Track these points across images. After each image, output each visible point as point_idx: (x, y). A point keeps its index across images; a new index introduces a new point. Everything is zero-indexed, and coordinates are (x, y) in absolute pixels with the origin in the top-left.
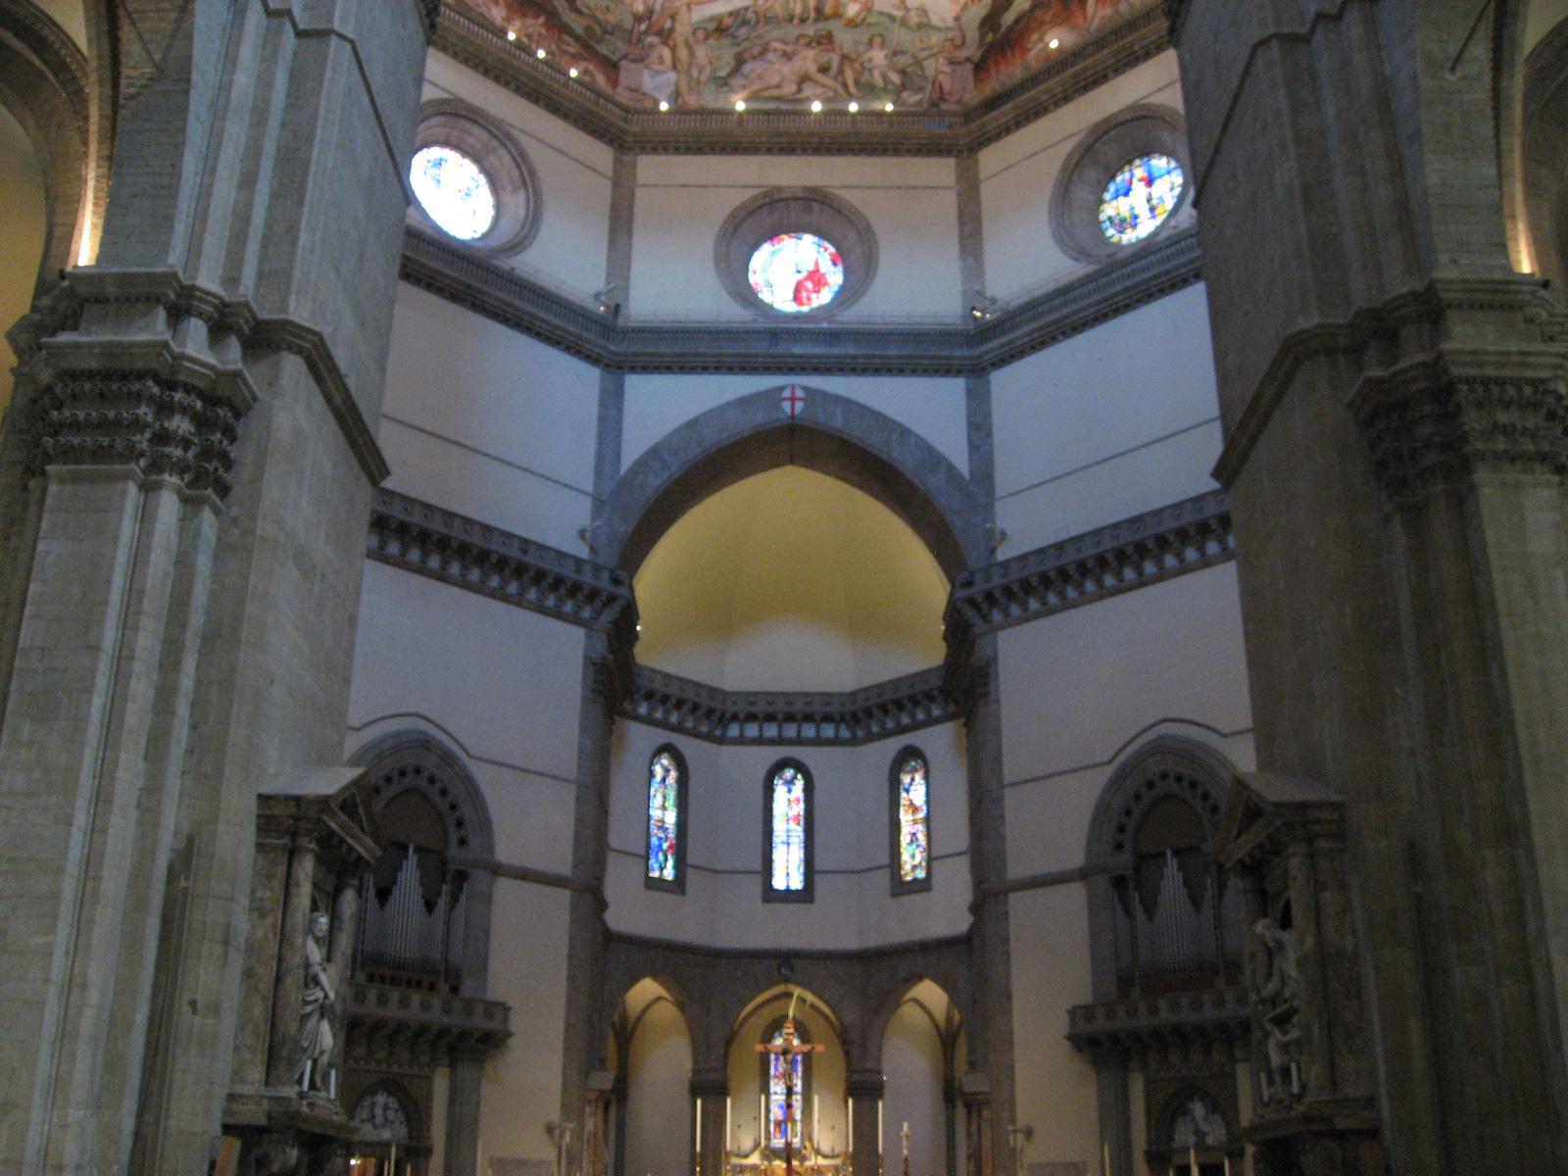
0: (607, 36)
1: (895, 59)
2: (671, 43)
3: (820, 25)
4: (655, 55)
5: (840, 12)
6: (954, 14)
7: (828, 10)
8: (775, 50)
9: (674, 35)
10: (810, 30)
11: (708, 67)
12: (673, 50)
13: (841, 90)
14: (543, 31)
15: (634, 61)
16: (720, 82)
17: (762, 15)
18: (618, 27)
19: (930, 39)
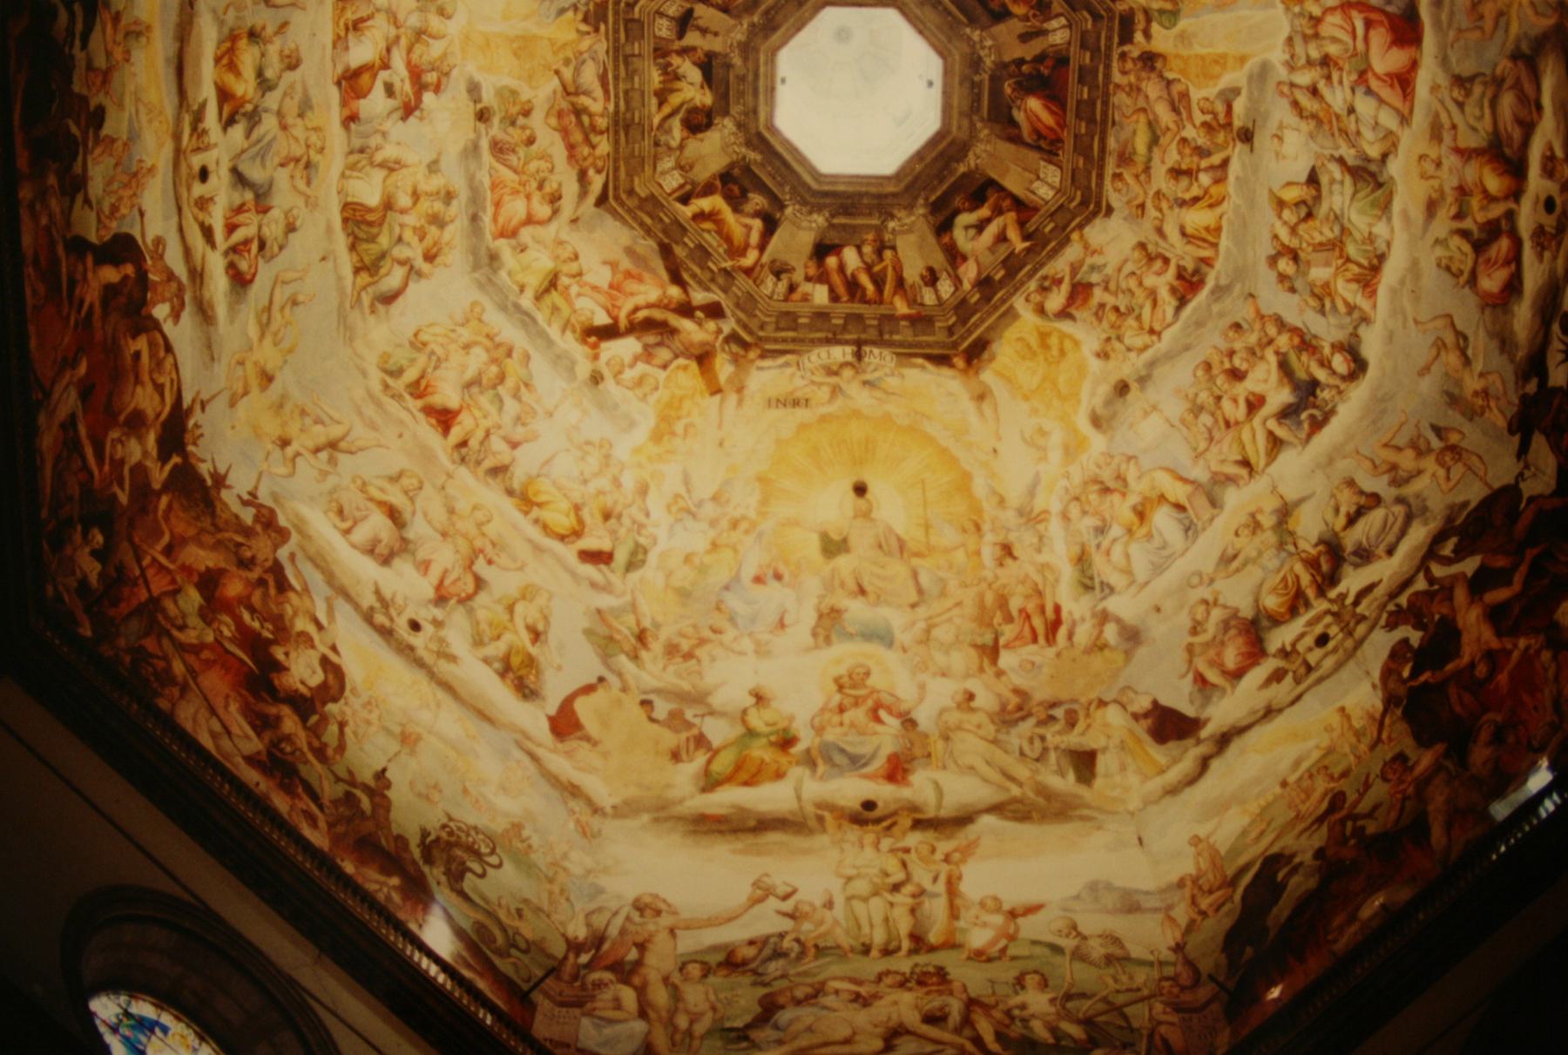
0: (513, 951)
1: (1070, 1005)
2: (637, 980)
3: (922, 959)
4: (606, 996)
5: (959, 938)
6: (1173, 944)
7: (933, 937)
8: (837, 992)
9: (643, 971)
10: (903, 964)
11: (710, 1015)
12: (641, 991)
13: (969, 1046)
14: (396, 897)
15: (562, 1004)
16: (733, 1035)
17: (810, 944)
18: (533, 948)
19: (1131, 978)
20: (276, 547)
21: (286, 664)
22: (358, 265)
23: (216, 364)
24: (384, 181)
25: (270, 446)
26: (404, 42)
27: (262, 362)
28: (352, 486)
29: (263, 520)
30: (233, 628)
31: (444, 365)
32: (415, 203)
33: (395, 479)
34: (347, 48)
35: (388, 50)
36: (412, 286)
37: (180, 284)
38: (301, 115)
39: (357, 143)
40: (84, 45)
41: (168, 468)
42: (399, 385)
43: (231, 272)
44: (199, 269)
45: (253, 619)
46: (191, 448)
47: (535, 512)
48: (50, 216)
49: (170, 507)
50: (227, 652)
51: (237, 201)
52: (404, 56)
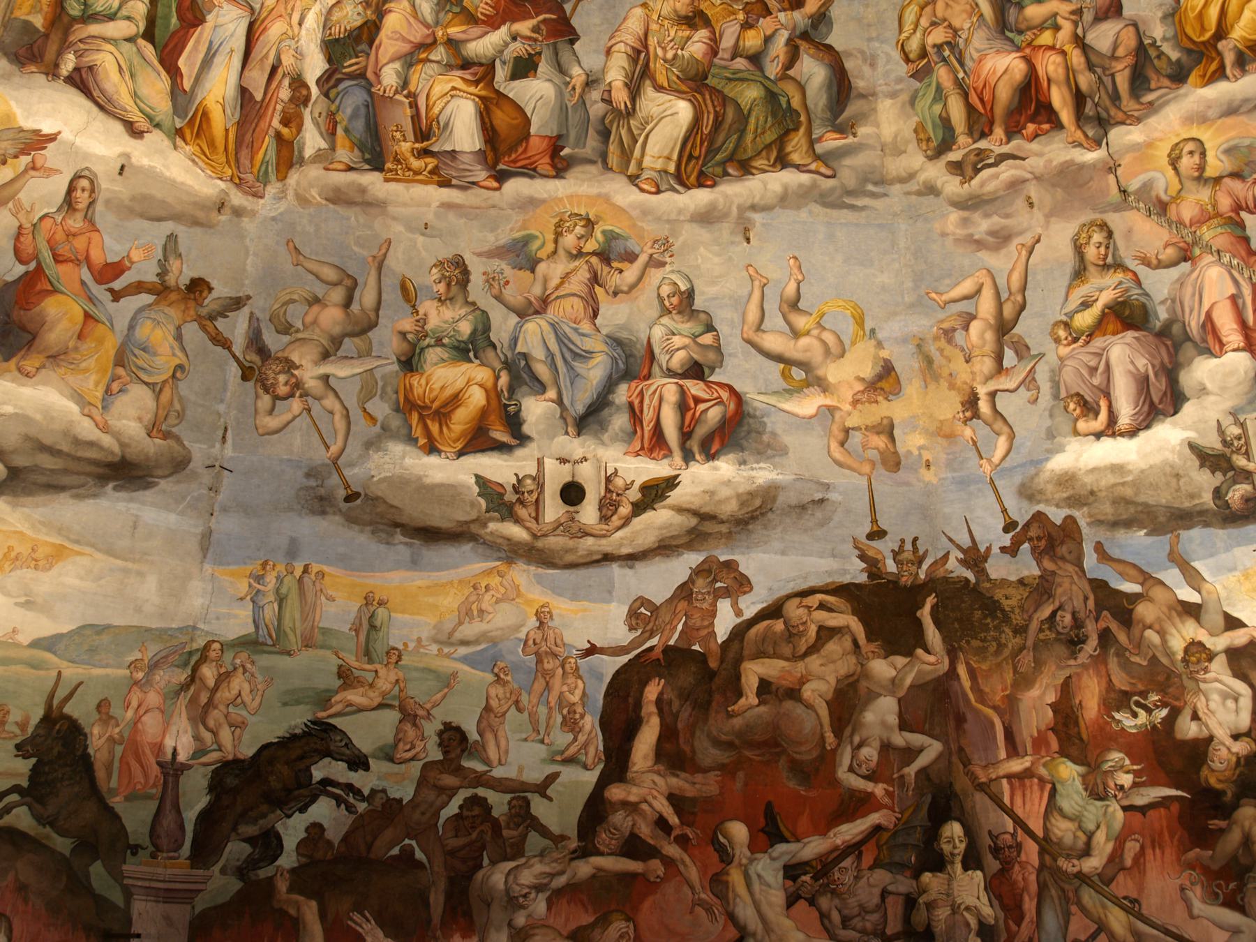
20: (1079, 563)
21: (1205, 733)
22: (774, 154)
23: (833, 496)
24: (659, 88)
25: (968, 432)
26: (455, 31)
27: (859, 387)
28: (1064, 351)
29: (1043, 543)
30: (1127, 762)
31: (961, 42)
32: (707, 22)
33: (1080, 273)
34: (453, 154)
35: (466, 65)
36: (836, 39)
37: (698, 572)
38: (532, 265)
39: (592, 142)
40: (358, 762)
41: (932, 634)
42: (963, 147)
43: (715, 447)
44: (694, 521)
45: (1135, 715)
46: (922, 576)
47: (1227, 48)
48: (539, 888)
49: (972, 673)
50: (1143, 810)
51: (620, 421)
52: (476, 31)
